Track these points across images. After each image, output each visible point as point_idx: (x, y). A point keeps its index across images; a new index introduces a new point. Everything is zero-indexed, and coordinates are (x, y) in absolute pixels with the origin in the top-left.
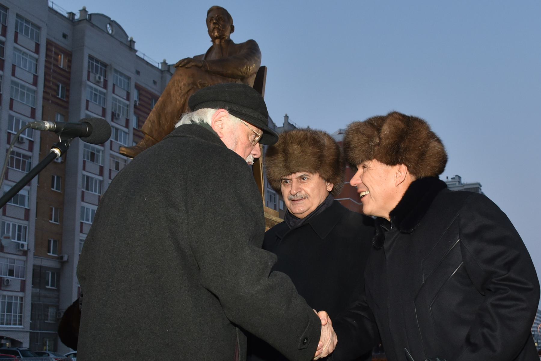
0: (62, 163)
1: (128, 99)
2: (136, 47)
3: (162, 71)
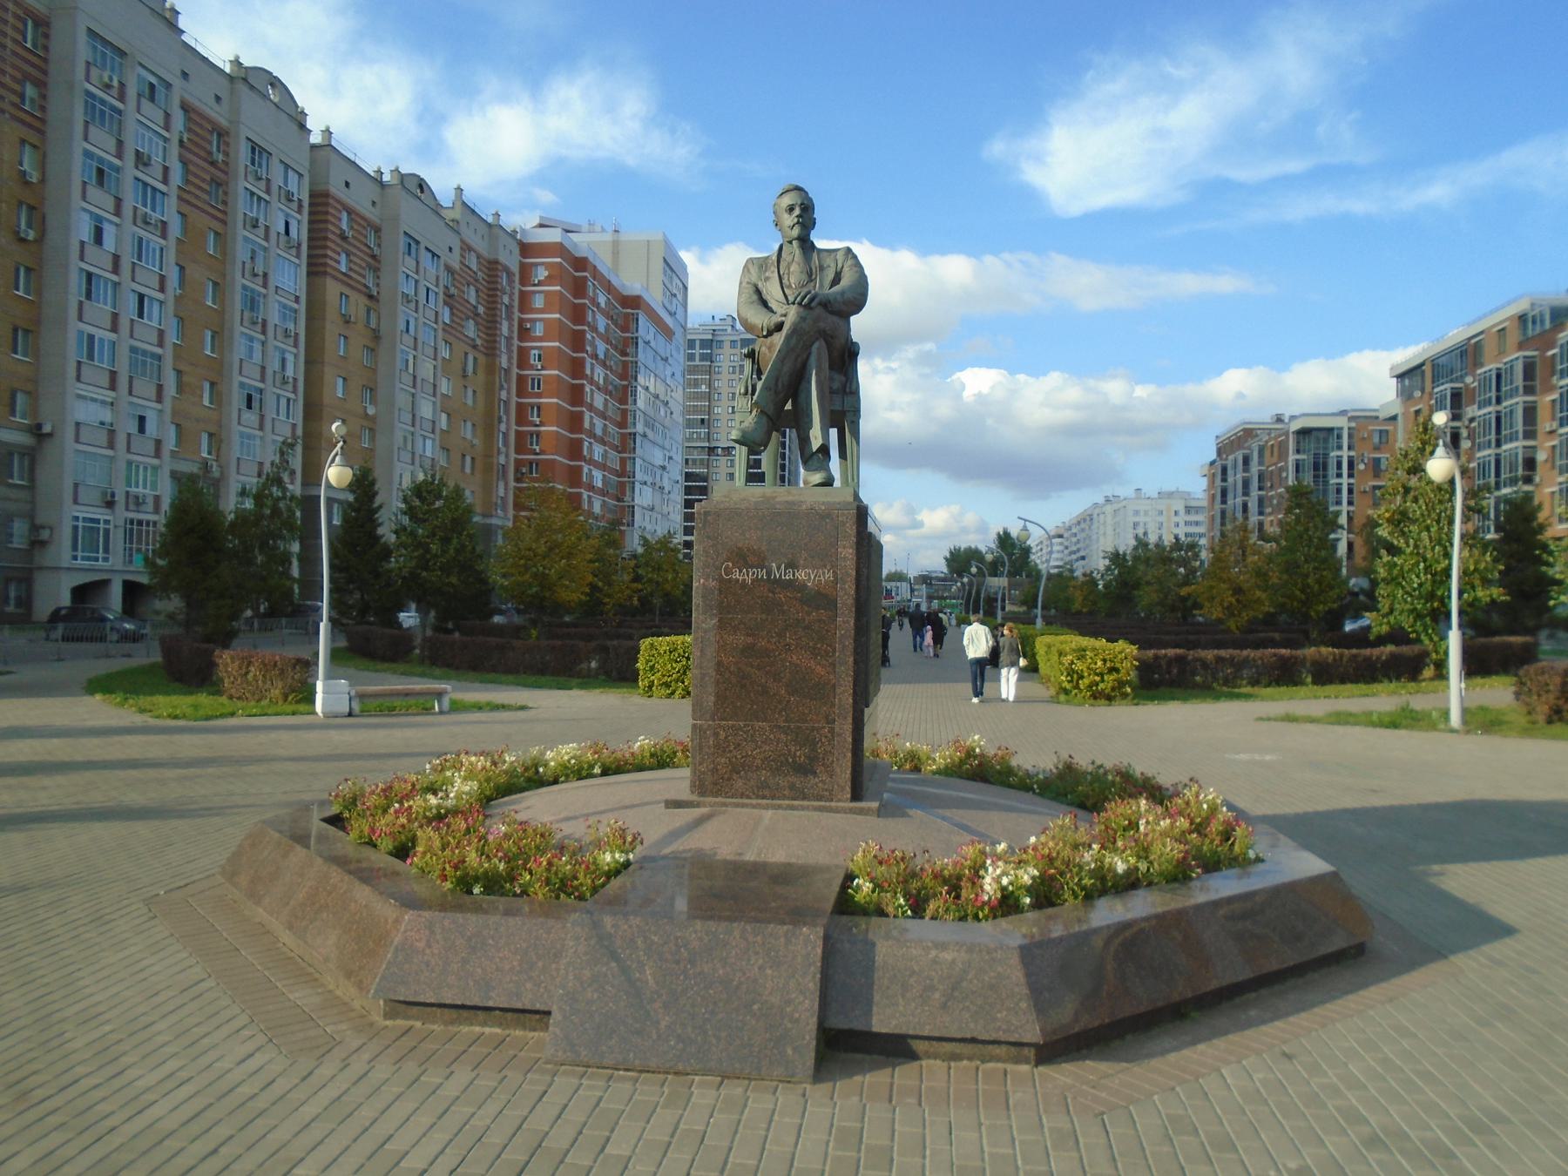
0: (36, 241)
1: (167, 128)
2: (182, 24)
3: (230, 78)
